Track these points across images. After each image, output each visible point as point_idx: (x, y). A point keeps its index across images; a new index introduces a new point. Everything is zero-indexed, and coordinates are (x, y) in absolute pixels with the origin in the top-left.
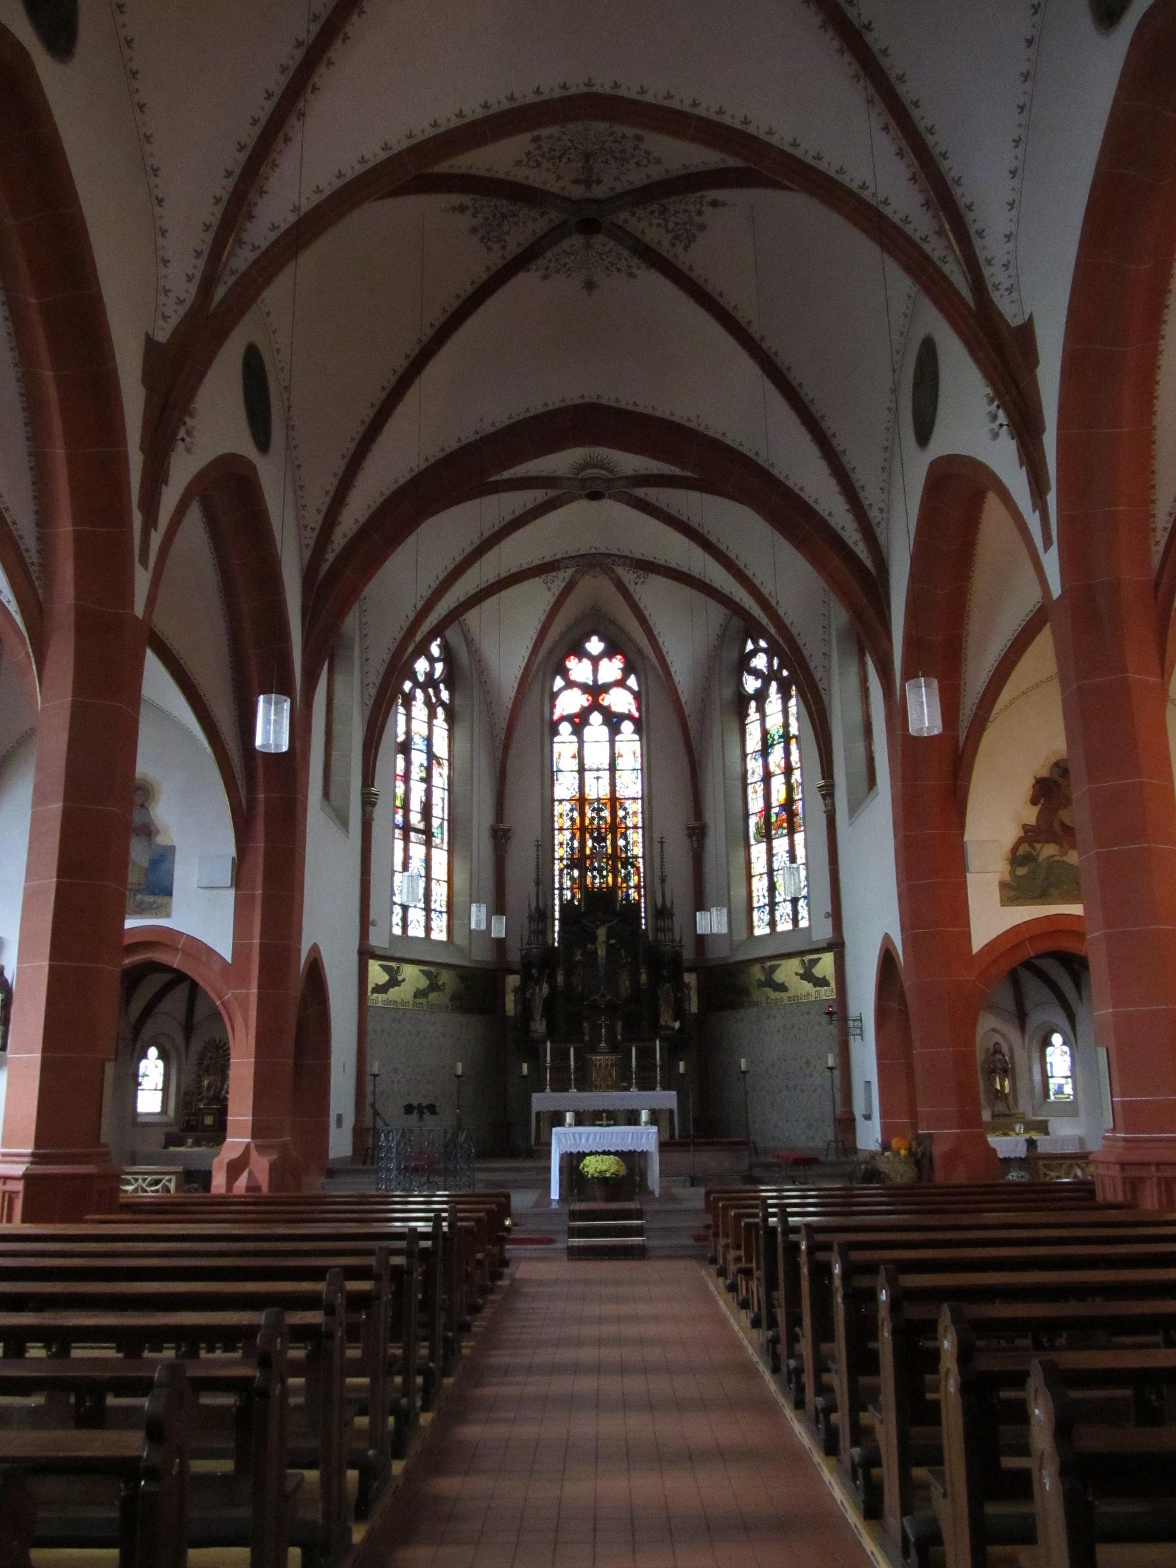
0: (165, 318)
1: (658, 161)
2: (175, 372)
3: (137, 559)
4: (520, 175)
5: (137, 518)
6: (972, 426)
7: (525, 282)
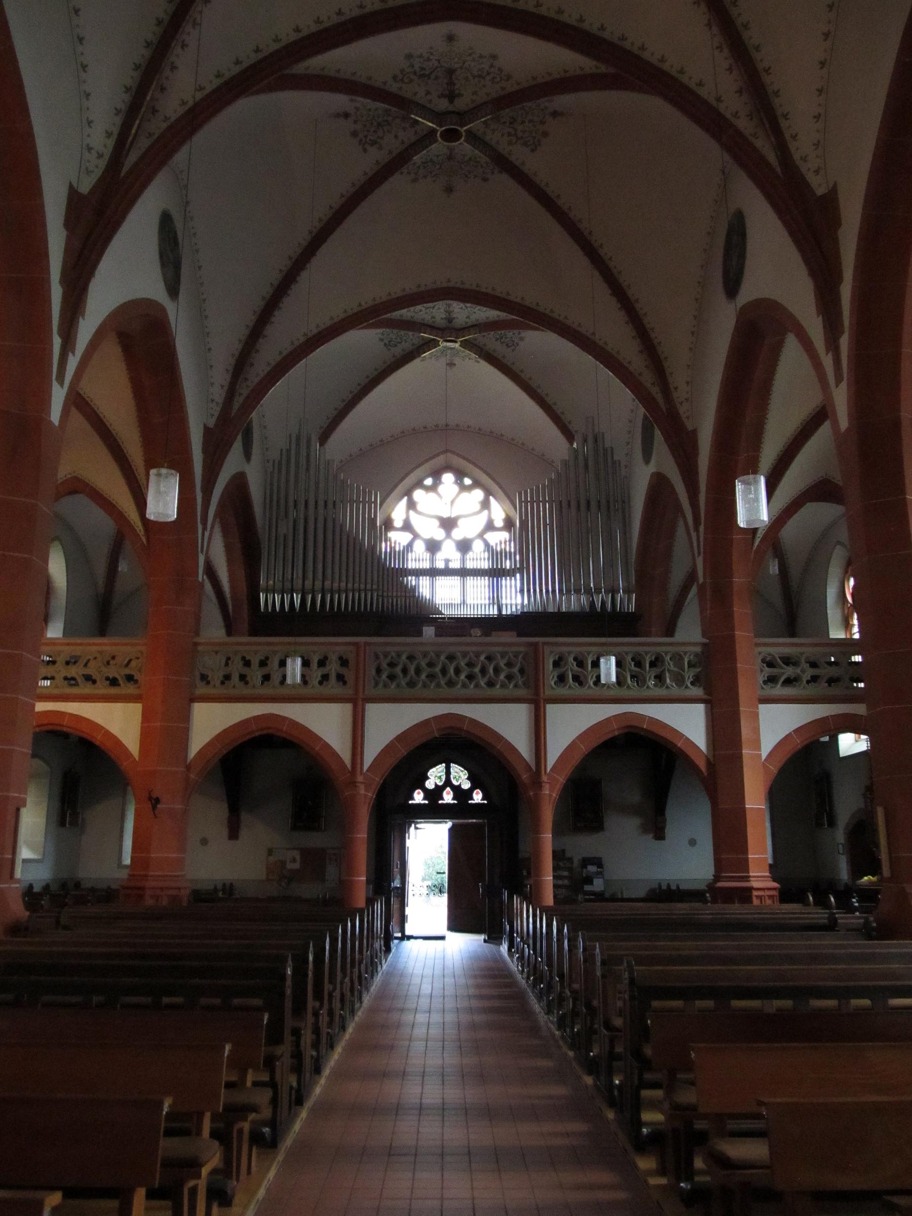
0: (88, 172)
1: (509, 77)
2: (96, 219)
3: (54, 377)
4: (393, 87)
5: (57, 342)
6: (776, 271)
7: (398, 181)
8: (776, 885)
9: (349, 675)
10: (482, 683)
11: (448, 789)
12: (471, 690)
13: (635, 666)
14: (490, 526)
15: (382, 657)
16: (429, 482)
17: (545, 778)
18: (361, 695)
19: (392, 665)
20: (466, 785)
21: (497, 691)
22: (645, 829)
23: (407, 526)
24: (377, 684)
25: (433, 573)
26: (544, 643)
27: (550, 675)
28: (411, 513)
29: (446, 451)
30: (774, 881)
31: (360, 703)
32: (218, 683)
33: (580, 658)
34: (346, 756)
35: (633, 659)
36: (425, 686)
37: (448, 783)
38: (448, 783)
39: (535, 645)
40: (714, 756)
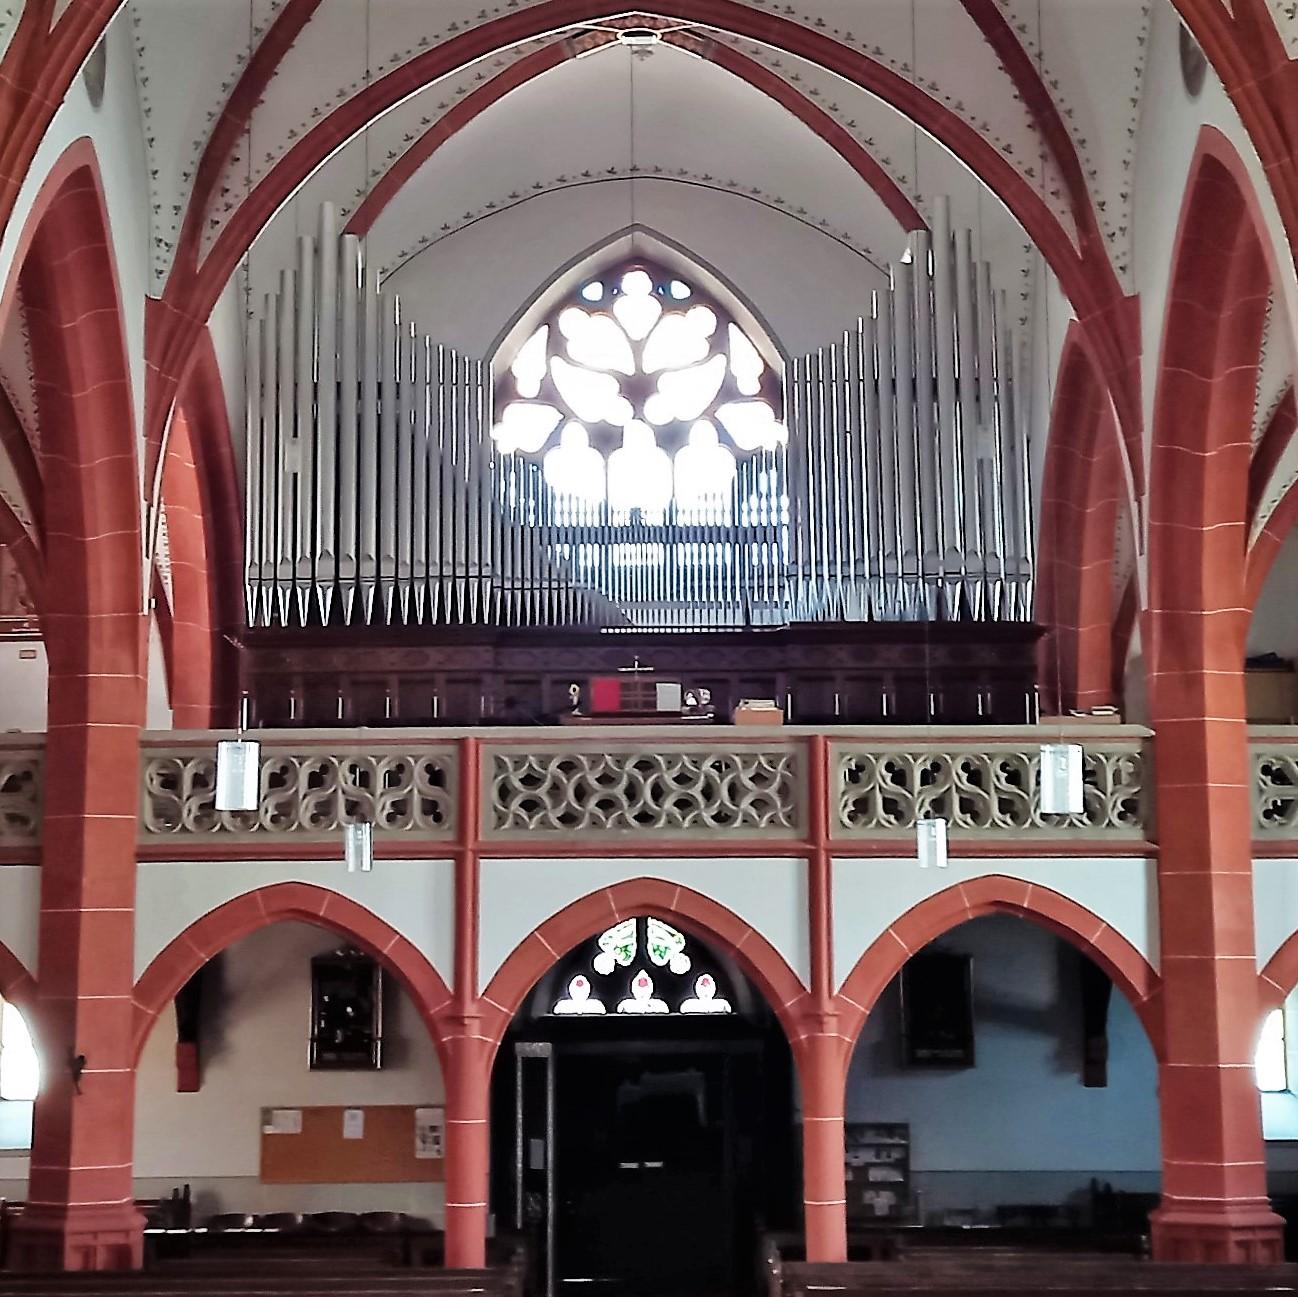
8: (1281, 1220)
9: (447, 799)
10: (707, 817)
11: (643, 974)
12: (685, 832)
13: (1008, 780)
14: (728, 392)
15: (510, 765)
16: (593, 292)
17: (828, 1006)
18: (470, 844)
19: (530, 780)
20: (681, 965)
21: (735, 833)
22: (1059, 1062)
23: (548, 395)
24: (501, 819)
25: (605, 536)
26: (827, 737)
27: (839, 795)
28: (556, 361)
29: (634, 227)
30: (1275, 1211)
31: (470, 855)
32: (188, 821)
33: (899, 764)
34: (435, 949)
35: (1003, 767)
36: (595, 823)
37: (642, 960)
38: (642, 960)
39: (811, 741)
40: (1163, 962)
